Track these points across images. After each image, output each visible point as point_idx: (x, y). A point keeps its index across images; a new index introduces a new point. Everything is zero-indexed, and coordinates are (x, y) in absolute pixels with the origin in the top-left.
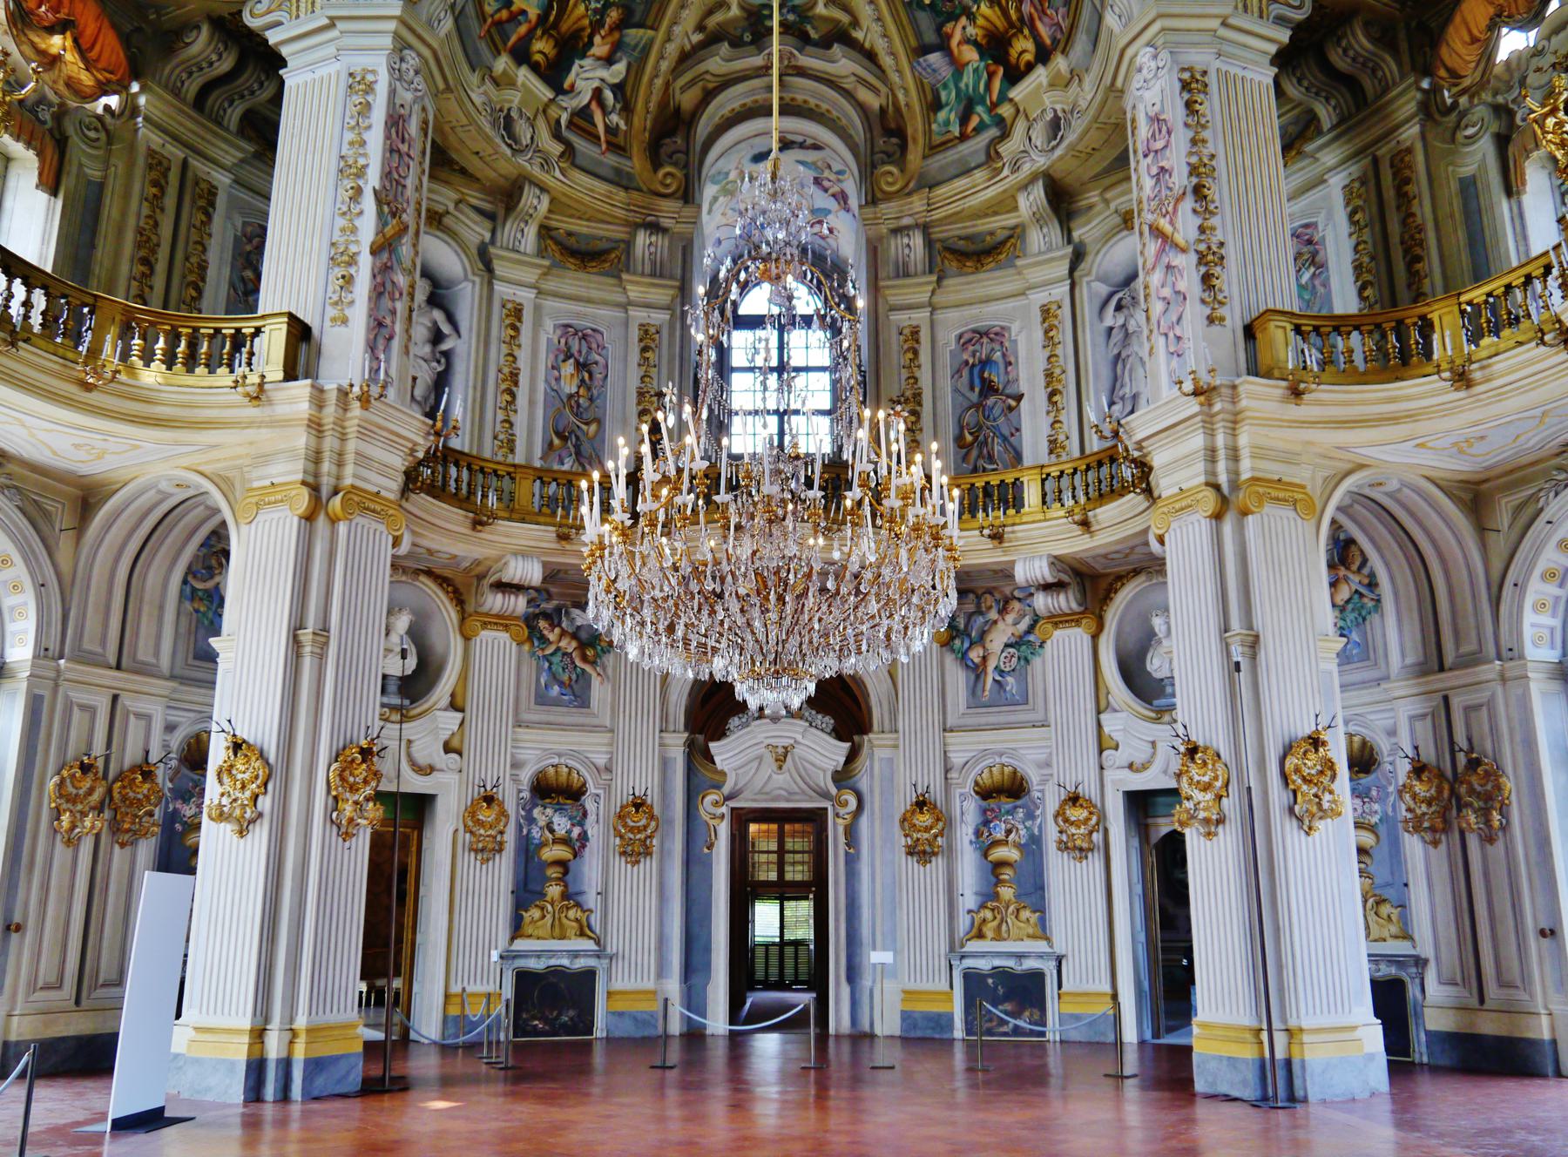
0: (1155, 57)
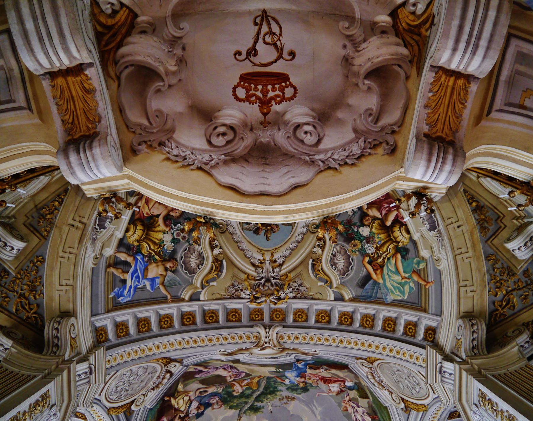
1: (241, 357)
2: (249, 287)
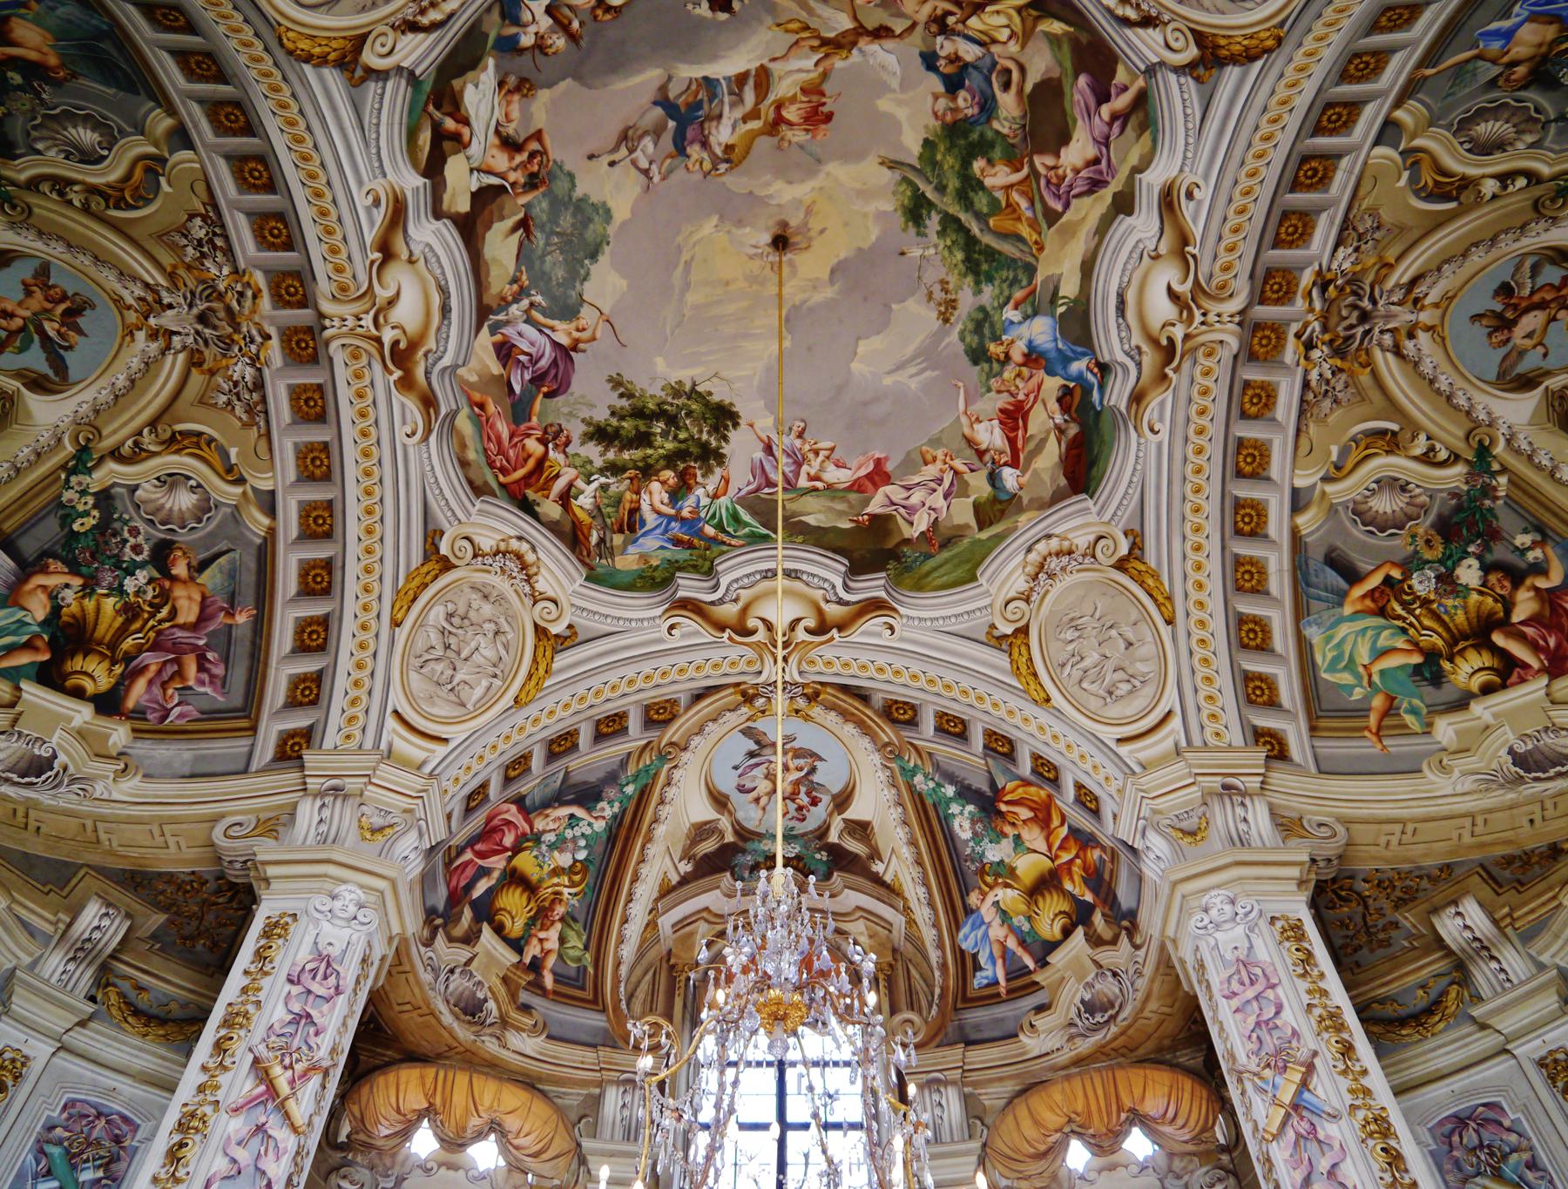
0: (361, 906)
1: (1143, 225)
2: (1358, 268)
